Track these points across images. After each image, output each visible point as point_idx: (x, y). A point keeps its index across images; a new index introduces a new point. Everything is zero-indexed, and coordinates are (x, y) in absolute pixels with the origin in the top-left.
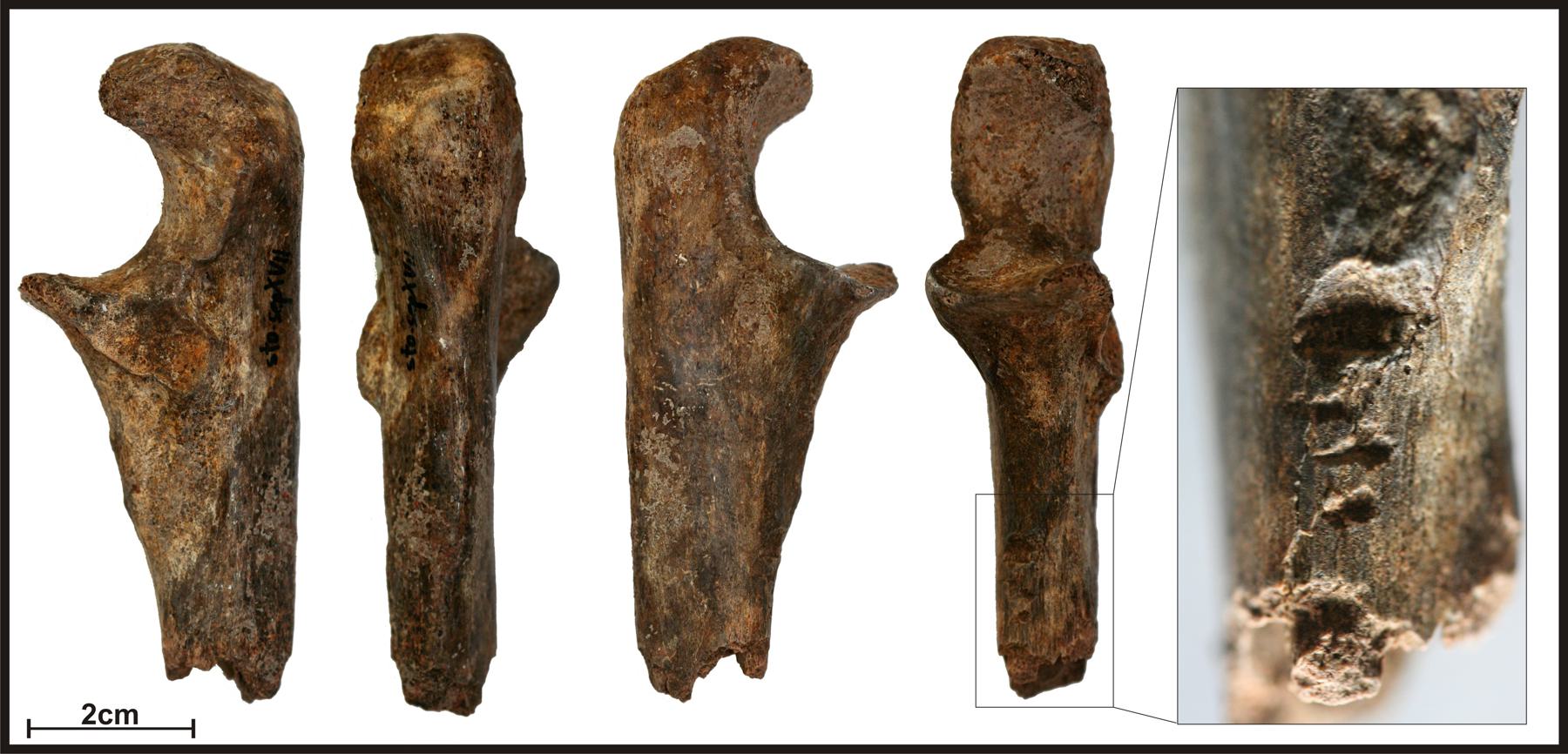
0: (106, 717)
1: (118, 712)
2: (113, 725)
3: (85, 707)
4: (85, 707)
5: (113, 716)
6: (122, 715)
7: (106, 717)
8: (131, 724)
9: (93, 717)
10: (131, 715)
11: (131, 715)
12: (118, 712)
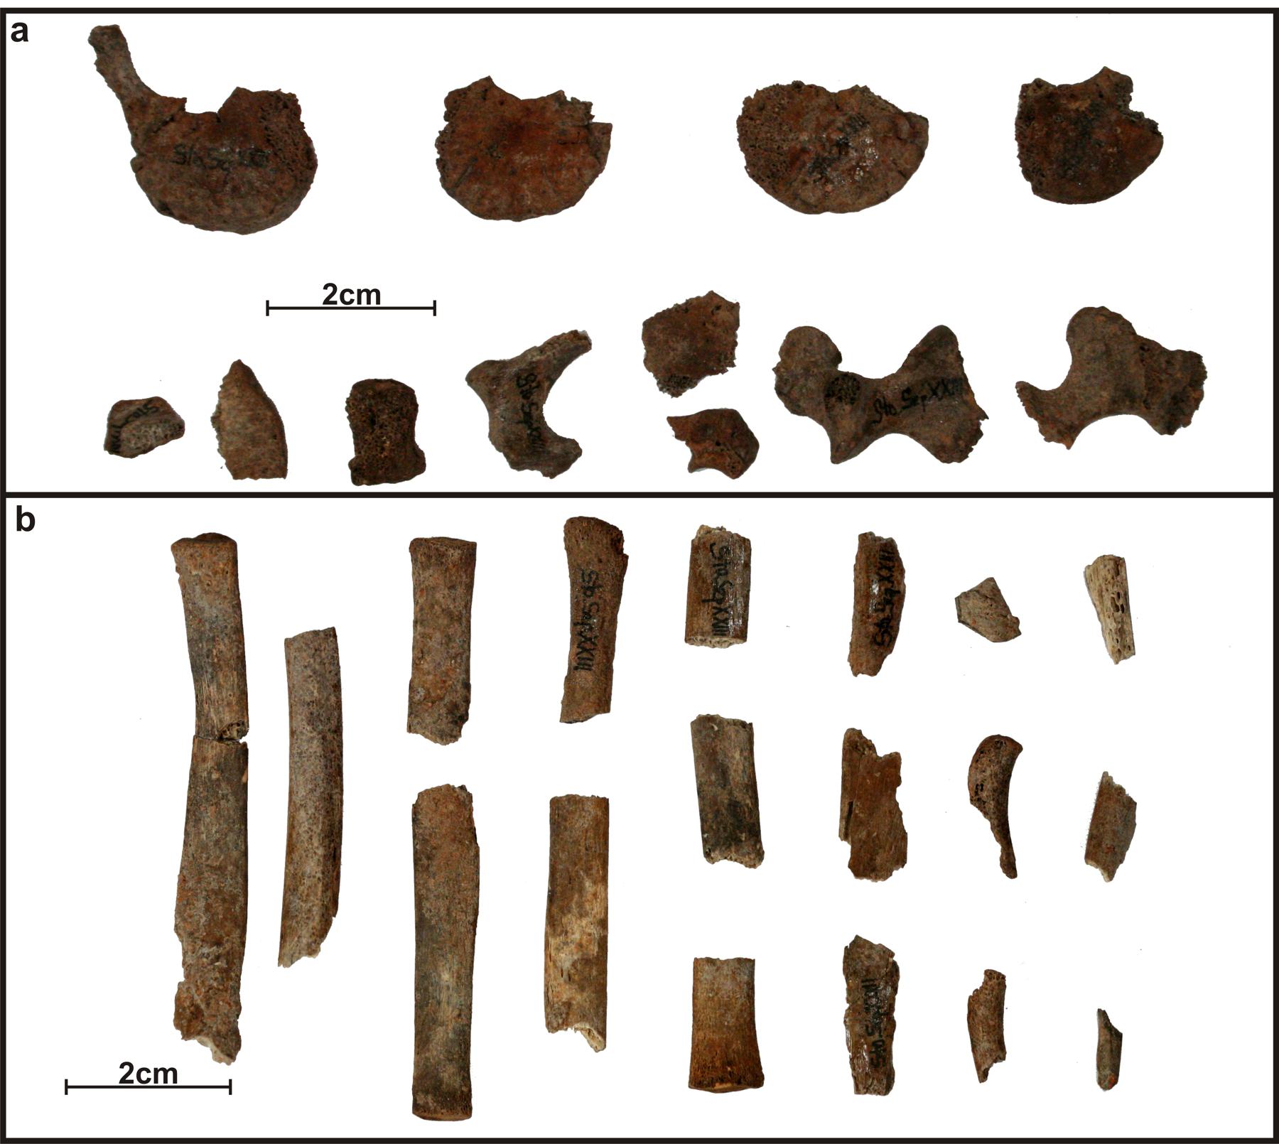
1: (360, 292)
2: (355, 304)
5: (355, 296)
8: (373, 304)
9: (335, 299)
11: (373, 295)
12: (360, 292)
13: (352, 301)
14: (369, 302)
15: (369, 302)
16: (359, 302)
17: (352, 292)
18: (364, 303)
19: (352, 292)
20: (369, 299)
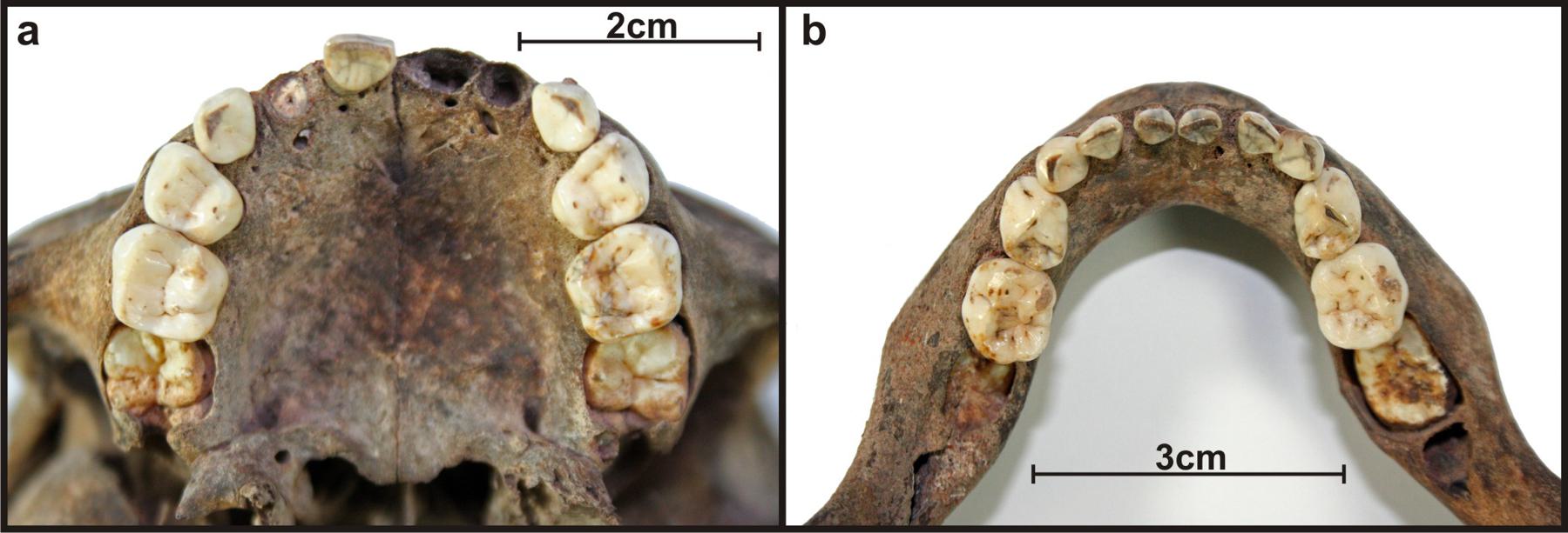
0: (1186, 460)
1: (1200, 455)
2: (1194, 469)
3: (1160, 448)
4: (1160, 448)
5: (1194, 460)
6: (1206, 458)
7: (1186, 460)
8: (1217, 469)
10: (1217, 458)
11: (1217, 458)
12: (1200, 455)
13: (1191, 465)
14: (1211, 467)
15: (1211, 467)
16: (1200, 467)
17: (1190, 454)
18: (1206, 469)
19: (1190, 454)
20: (1212, 462)
